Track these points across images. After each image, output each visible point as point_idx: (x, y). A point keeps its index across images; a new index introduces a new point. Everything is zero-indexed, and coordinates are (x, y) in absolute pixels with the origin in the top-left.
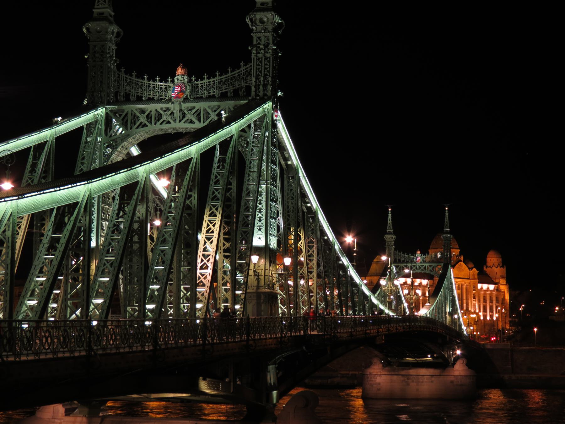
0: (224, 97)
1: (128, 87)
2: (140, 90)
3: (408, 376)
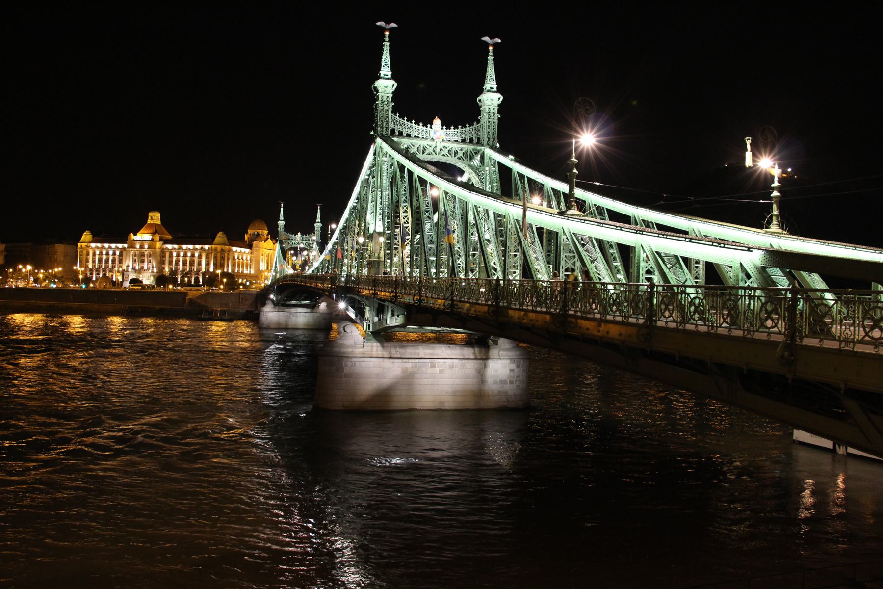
0: (463, 141)
1: (401, 128)
2: (409, 130)
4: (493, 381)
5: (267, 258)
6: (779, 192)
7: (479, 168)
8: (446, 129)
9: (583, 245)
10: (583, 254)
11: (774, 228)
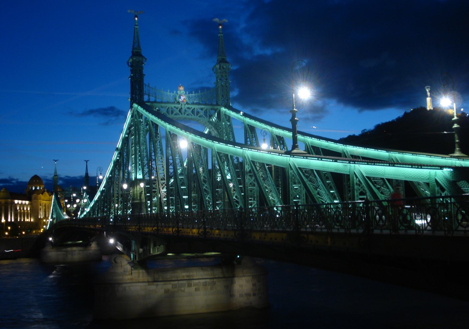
3: (67, 251)
4: (240, 295)
5: (44, 208)
6: (458, 124)
7: (217, 123)
8: (189, 93)
9: (307, 177)
10: (308, 183)
11: (457, 154)
